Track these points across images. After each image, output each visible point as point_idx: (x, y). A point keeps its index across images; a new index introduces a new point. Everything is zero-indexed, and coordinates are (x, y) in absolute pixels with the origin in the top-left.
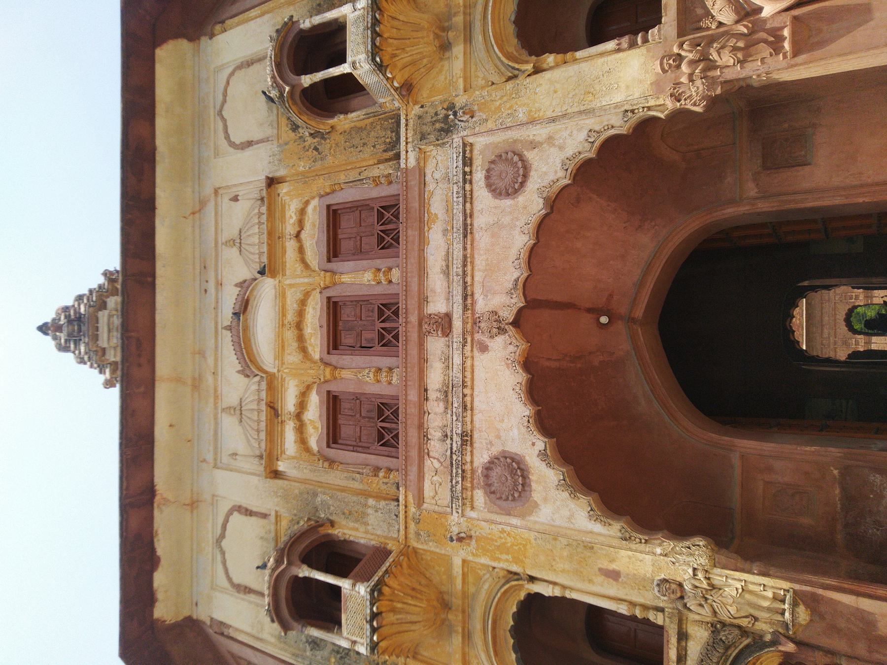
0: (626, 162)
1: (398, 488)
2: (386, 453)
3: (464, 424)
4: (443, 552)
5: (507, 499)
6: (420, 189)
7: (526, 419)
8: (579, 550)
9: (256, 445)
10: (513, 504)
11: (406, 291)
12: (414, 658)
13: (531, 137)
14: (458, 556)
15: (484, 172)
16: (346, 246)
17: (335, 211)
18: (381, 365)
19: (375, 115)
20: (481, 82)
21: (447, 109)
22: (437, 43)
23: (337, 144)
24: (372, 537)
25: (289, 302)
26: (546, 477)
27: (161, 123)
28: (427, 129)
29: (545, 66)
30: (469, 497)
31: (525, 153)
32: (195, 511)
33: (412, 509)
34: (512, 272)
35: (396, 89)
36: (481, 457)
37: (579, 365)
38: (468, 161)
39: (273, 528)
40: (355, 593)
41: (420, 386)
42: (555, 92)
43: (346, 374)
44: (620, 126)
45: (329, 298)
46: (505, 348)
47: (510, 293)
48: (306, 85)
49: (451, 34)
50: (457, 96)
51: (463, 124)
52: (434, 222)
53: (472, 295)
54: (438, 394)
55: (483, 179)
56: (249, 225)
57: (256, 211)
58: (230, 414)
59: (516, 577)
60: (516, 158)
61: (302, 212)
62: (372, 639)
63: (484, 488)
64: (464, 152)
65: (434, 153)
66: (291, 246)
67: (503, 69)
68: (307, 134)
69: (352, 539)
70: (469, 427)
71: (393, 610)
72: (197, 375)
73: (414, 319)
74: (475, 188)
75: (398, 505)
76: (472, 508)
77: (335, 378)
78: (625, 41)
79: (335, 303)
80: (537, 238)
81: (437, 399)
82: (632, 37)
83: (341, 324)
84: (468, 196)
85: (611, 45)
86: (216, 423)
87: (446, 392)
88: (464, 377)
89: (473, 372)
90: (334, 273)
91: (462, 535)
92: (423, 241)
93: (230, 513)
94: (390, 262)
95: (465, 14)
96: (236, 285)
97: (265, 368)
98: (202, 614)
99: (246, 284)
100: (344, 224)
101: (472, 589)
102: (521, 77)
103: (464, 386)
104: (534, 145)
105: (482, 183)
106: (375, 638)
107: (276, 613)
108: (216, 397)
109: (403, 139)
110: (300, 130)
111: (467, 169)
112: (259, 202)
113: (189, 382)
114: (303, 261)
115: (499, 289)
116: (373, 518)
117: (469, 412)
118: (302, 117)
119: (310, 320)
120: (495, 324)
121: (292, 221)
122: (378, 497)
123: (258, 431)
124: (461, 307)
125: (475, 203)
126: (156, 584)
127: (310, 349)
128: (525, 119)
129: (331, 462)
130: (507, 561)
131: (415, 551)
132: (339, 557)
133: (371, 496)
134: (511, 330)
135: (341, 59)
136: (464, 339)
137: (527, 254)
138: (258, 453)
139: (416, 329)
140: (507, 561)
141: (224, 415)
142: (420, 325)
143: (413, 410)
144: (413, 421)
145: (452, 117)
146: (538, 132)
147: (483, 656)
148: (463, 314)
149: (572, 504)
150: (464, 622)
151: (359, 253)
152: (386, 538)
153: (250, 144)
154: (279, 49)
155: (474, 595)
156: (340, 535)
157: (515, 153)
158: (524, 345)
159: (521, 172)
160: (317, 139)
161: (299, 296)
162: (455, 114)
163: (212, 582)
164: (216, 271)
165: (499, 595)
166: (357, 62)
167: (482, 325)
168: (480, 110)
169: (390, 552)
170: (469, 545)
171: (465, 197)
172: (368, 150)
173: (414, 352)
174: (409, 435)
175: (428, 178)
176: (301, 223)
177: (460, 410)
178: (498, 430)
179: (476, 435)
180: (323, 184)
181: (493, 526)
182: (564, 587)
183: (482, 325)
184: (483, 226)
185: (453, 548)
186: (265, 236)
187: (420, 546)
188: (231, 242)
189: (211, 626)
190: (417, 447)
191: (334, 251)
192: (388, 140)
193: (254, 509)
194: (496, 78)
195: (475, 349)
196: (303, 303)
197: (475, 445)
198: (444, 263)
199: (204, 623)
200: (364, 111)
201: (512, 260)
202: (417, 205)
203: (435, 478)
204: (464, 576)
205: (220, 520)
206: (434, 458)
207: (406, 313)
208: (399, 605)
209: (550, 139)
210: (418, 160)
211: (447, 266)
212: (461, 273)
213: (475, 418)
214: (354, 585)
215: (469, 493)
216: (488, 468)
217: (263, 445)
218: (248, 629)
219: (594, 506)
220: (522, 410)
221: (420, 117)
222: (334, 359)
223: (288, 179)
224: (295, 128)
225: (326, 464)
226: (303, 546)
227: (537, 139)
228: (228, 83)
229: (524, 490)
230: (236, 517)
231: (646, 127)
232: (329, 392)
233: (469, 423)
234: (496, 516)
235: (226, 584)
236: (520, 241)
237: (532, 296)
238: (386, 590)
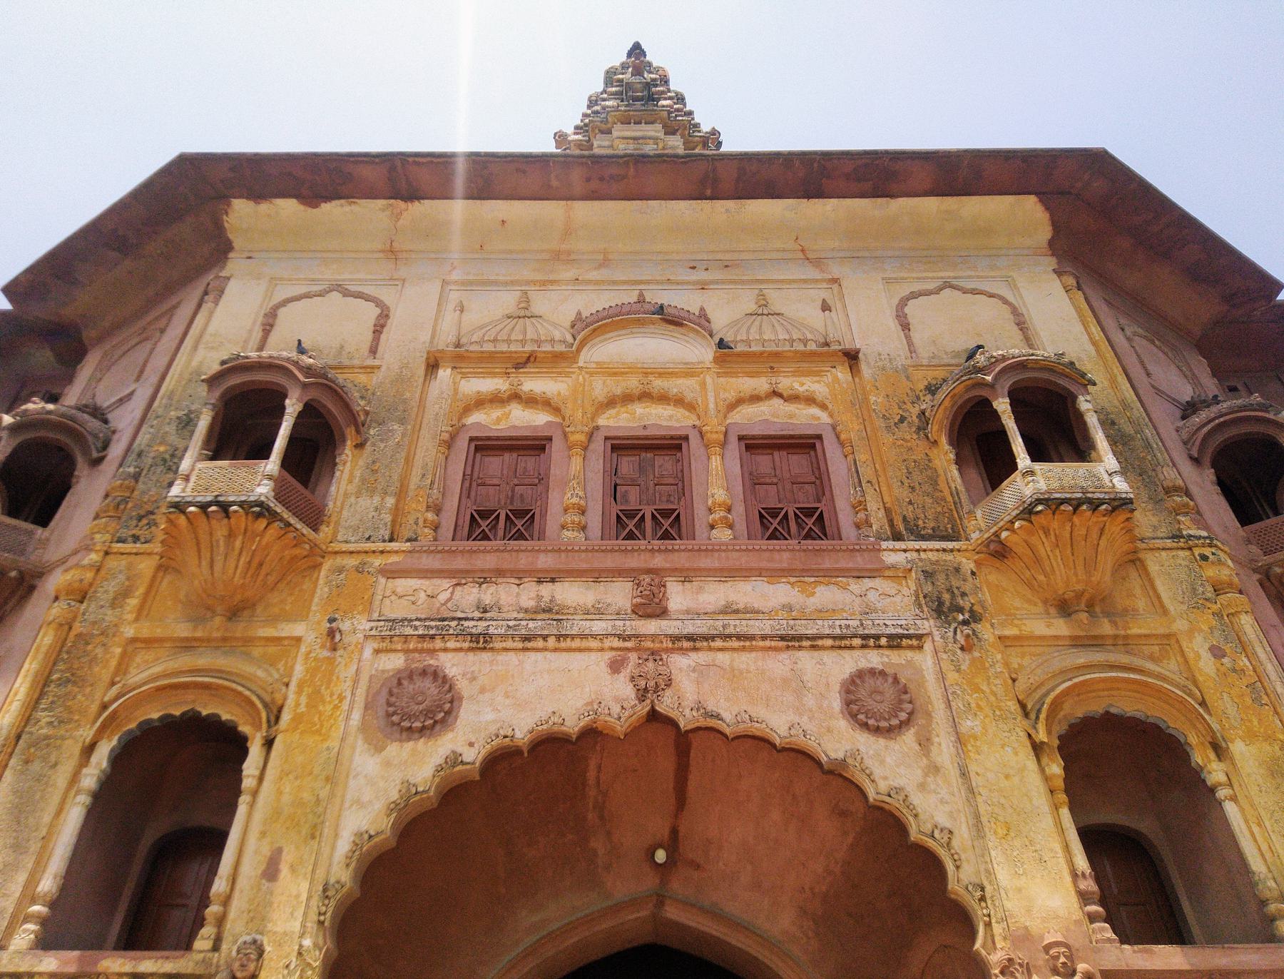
1: (409, 540)
2: (460, 522)
3: (503, 637)
4: (314, 608)
5: (389, 704)
6: (849, 570)
7: (510, 733)
8: (310, 816)
9: (475, 338)
10: (381, 713)
11: (700, 550)
12: (160, 567)
13: (936, 740)
14: (307, 631)
15: (881, 667)
16: (764, 462)
17: (813, 446)
18: (589, 513)
19: (957, 504)
20: (1015, 662)
21: (971, 611)
22: (1069, 595)
23: (910, 449)
24: (339, 504)
25: (680, 381)
26: (420, 765)
27: (931, 205)
28: (941, 578)
29: (1045, 760)
30: (393, 647)
31: (912, 731)
32: (381, 255)
33: (377, 562)
34: (731, 710)
35: (997, 534)
36: (453, 664)
37: (590, 816)
38: (895, 642)
39: (356, 362)
40: (260, 479)
41: (559, 571)
42: (1007, 777)
43: (576, 463)
44: (960, 880)
45: (686, 438)
46: (616, 699)
47: (699, 706)
48: (995, 404)
49: (1083, 616)
50: (992, 625)
51: (951, 634)
52: (802, 592)
53: (695, 649)
54: (547, 599)
55: (870, 666)
56: (789, 327)
57: (809, 336)
58: (520, 303)
59: (272, 719)
60: (903, 716)
61: (810, 400)
62: (190, 504)
63: (406, 669)
64: (909, 637)
65: (905, 591)
66: (761, 384)
67: (1037, 696)
68: (923, 407)
69: (338, 474)
70: (498, 645)
71: (231, 535)
72: (573, 257)
73: (658, 561)
74: (857, 653)
75: (384, 541)
76: (377, 651)
77: (570, 448)
78: (1089, 885)
79: (679, 448)
80: (784, 750)
81: (540, 598)
82: (1097, 897)
83: (649, 455)
84: (843, 643)
85: (1082, 863)
86: (506, 283)
87: (549, 610)
88: (573, 637)
89: (580, 650)
90: (724, 445)
91: (338, 637)
92: (774, 574)
93: (378, 302)
94: (741, 527)
95: (1116, 637)
96: (702, 309)
97: (585, 349)
98: (235, 265)
99: (703, 322)
100: (794, 458)
101: (257, 652)
102: (1026, 723)
103: (559, 637)
104: (925, 743)
105: (863, 664)
106: (192, 509)
107: (234, 367)
108: (544, 283)
109: (924, 545)
110: (929, 397)
111: (883, 641)
112: (822, 340)
113: (563, 247)
114: (740, 402)
116: (367, 504)
117: (520, 645)
118: (948, 399)
119: (653, 412)
120: (652, 683)
121: (796, 385)
122: (397, 512)
123: (495, 341)
124: (677, 632)
125: (834, 653)
126: (280, 202)
127: (612, 412)
128: (963, 730)
129: (449, 444)
130: (298, 705)
131: (317, 567)
132: (312, 455)
133: (398, 501)
134: (644, 709)
135: (1037, 454)
136: (629, 637)
137: (758, 734)
138: (464, 340)
139: (643, 565)
140: (298, 705)
141: (518, 293)
142: (649, 571)
143: (523, 561)
144: (506, 561)
145: (961, 617)
146: (944, 750)
147: (157, 669)
148: (666, 636)
149: (379, 806)
150: (209, 640)
151: (753, 482)
152: (337, 523)
153: (906, 327)
154: (1045, 366)
155: (248, 654)
156: (344, 457)
157: (911, 714)
158: (620, 728)
159: (884, 724)
160: (917, 421)
161: (689, 397)
162: (965, 623)
163: (281, 279)
164: (723, 282)
165: (247, 693)
166: (1033, 478)
167: (651, 664)
168: (973, 660)
169: (316, 530)
170: (323, 646)
171: (842, 637)
172: (904, 494)
173: (610, 561)
174: (488, 556)
175: (868, 583)
176: (794, 398)
177: (523, 632)
178: (493, 690)
179: (485, 656)
180: (852, 429)
181: (349, 683)
182: (255, 793)
183: (651, 664)
184: (799, 666)
185: (319, 623)
186: (774, 348)
187: (323, 573)
188: (763, 302)
189: (217, 277)
190: (469, 567)
191: (753, 445)
192: (920, 522)
193: (383, 337)
194: (1022, 685)
195: (614, 653)
196: (679, 401)
197: (471, 655)
198: (741, 606)
199: (223, 268)
200: (961, 488)
201: (749, 710)
202: (827, 565)
203: (422, 595)
204: (277, 640)
205: (367, 290)
206: (452, 593)
207: (666, 550)
208: (238, 544)
209: (934, 769)
210: (893, 567)
211: (737, 612)
212: (727, 632)
213: (511, 654)
214: (270, 477)
215: (399, 647)
216: (436, 675)
217: (472, 348)
218: (211, 329)
219: (376, 840)
220: (523, 727)
221: (957, 570)
222: (598, 446)
223: (857, 380)
224: (932, 390)
225: (446, 436)
226: (330, 406)
227: (934, 749)
228: (991, 296)
229: (403, 730)
230: (372, 312)
231: (960, 920)
232: (550, 439)
233: (504, 645)
234: (365, 688)
235: (278, 297)
236: (779, 723)
237: (696, 741)
238: (262, 523)
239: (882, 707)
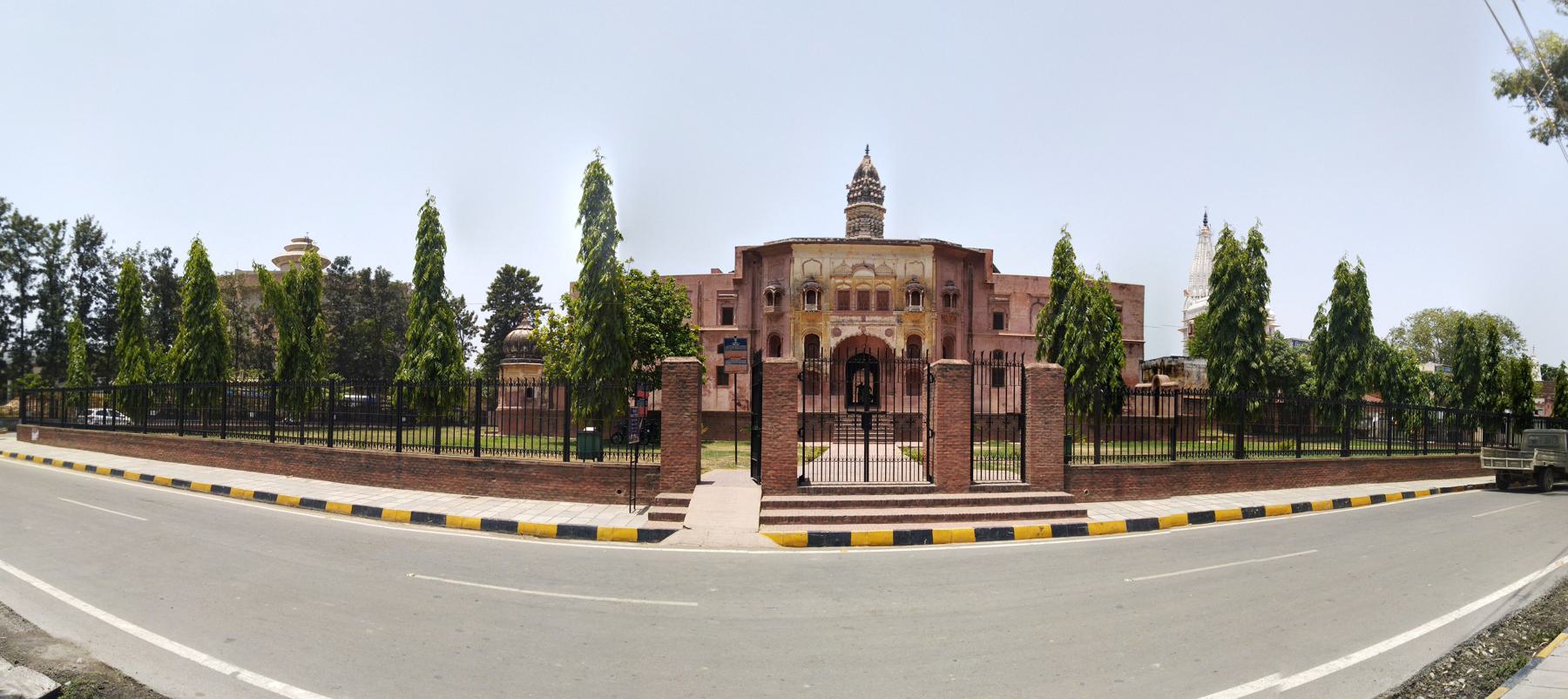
0: (888, 351)
26: (838, 339)
115: (870, 331)
239: (889, 333)
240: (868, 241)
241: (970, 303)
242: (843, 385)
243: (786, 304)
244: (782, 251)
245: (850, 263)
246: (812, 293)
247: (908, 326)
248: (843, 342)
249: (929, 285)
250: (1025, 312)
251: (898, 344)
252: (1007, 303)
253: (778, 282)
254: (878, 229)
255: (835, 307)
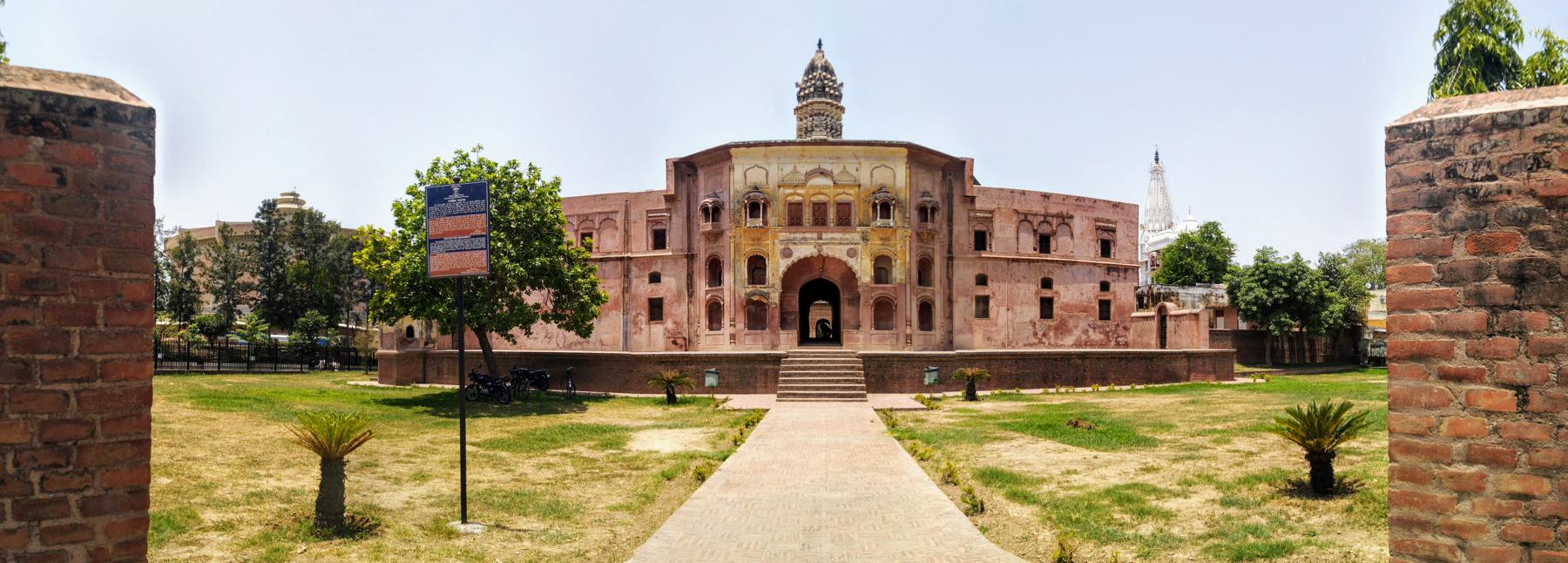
26: (789, 262)
115: (828, 251)
166: (879, 222)
239: (852, 253)
240: (824, 142)
241: (950, 220)
242: (795, 318)
243: (725, 219)
244: (720, 156)
245: (804, 168)
246: (755, 206)
247: (876, 244)
248: (794, 265)
249: (902, 196)
250: (1010, 232)
251: (864, 269)
252: (990, 220)
253: (715, 195)
254: (836, 130)
255: (785, 221)
